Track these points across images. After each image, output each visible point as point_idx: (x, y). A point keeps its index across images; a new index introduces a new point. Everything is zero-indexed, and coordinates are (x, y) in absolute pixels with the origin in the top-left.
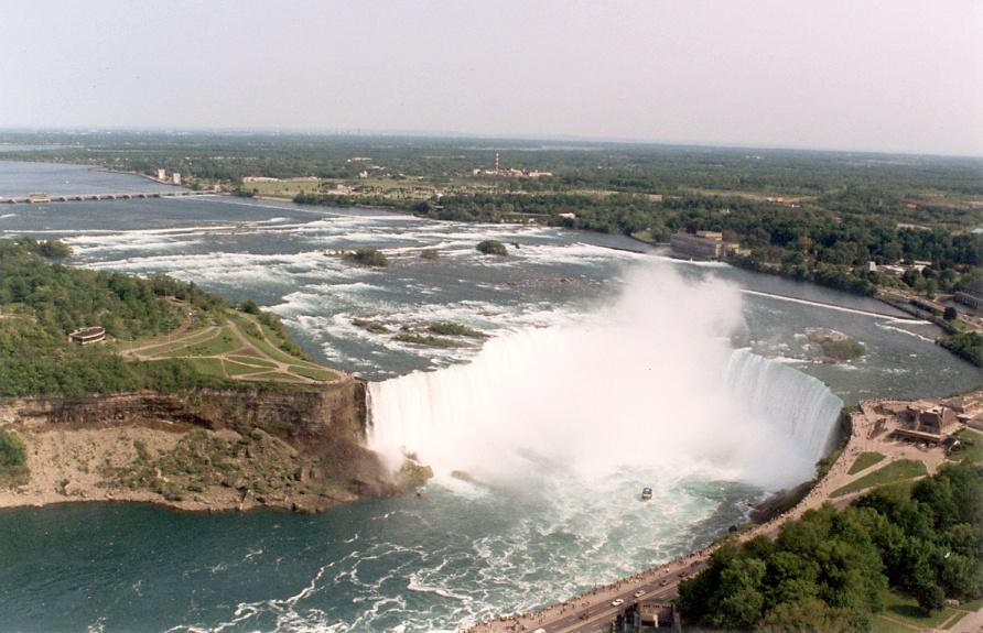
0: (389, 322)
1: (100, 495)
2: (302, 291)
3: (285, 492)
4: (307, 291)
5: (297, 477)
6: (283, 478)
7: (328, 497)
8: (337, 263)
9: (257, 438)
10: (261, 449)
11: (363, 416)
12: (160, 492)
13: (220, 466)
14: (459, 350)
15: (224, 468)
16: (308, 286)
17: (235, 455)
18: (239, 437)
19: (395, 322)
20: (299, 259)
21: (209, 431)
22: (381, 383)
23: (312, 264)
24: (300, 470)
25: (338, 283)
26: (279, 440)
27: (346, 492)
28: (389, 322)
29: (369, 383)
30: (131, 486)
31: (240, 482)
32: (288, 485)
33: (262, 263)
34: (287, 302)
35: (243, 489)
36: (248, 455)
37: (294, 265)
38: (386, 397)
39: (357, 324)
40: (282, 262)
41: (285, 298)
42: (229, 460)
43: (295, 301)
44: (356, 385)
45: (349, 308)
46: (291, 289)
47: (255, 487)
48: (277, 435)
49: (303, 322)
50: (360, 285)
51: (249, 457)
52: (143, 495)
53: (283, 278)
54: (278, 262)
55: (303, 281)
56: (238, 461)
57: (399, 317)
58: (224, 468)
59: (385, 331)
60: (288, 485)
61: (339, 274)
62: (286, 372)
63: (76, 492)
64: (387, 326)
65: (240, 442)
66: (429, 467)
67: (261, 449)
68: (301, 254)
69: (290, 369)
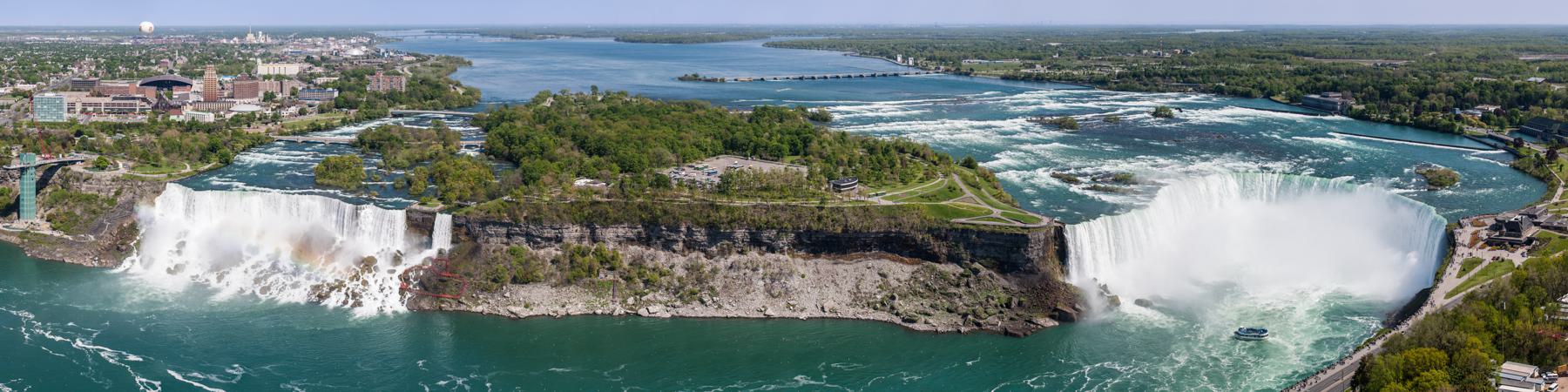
0: (1080, 175)
1: (849, 313)
2: (1011, 150)
3: (999, 318)
4: (1015, 150)
5: (1008, 306)
6: (996, 306)
7: (1034, 323)
8: (1038, 128)
9: (976, 272)
10: (978, 281)
11: (1063, 254)
12: (897, 314)
13: (947, 294)
14: (1138, 197)
15: (949, 296)
16: (1015, 146)
17: (958, 286)
18: (962, 270)
19: (1085, 175)
20: (1007, 125)
21: (937, 265)
22: (1076, 226)
23: (1018, 128)
24: (1010, 299)
25: (1040, 143)
26: (995, 275)
27: (1047, 319)
28: (1080, 175)
29: (1067, 226)
30: (875, 308)
31: (963, 309)
32: (1001, 312)
33: (979, 128)
34: (997, 159)
35: (965, 316)
36: (967, 285)
37: (1003, 129)
38: (1084, 238)
39: (1054, 176)
40: (994, 127)
41: (997, 155)
42: (953, 290)
43: (1004, 159)
44: (1056, 227)
45: (1046, 164)
46: (999, 151)
47: (974, 313)
48: (992, 268)
49: (1013, 176)
50: (1056, 144)
51: (970, 287)
52: (883, 316)
53: (993, 140)
54: (990, 127)
55: (1011, 142)
56: (962, 290)
57: (1089, 170)
58: (949, 296)
59: (1077, 182)
60: (1001, 312)
61: (1039, 136)
62: (999, 216)
63: (833, 310)
64: (1079, 178)
65: (962, 275)
66: (1116, 296)
67: (978, 281)
68: (1009, 121)
69: (1003, 214)
